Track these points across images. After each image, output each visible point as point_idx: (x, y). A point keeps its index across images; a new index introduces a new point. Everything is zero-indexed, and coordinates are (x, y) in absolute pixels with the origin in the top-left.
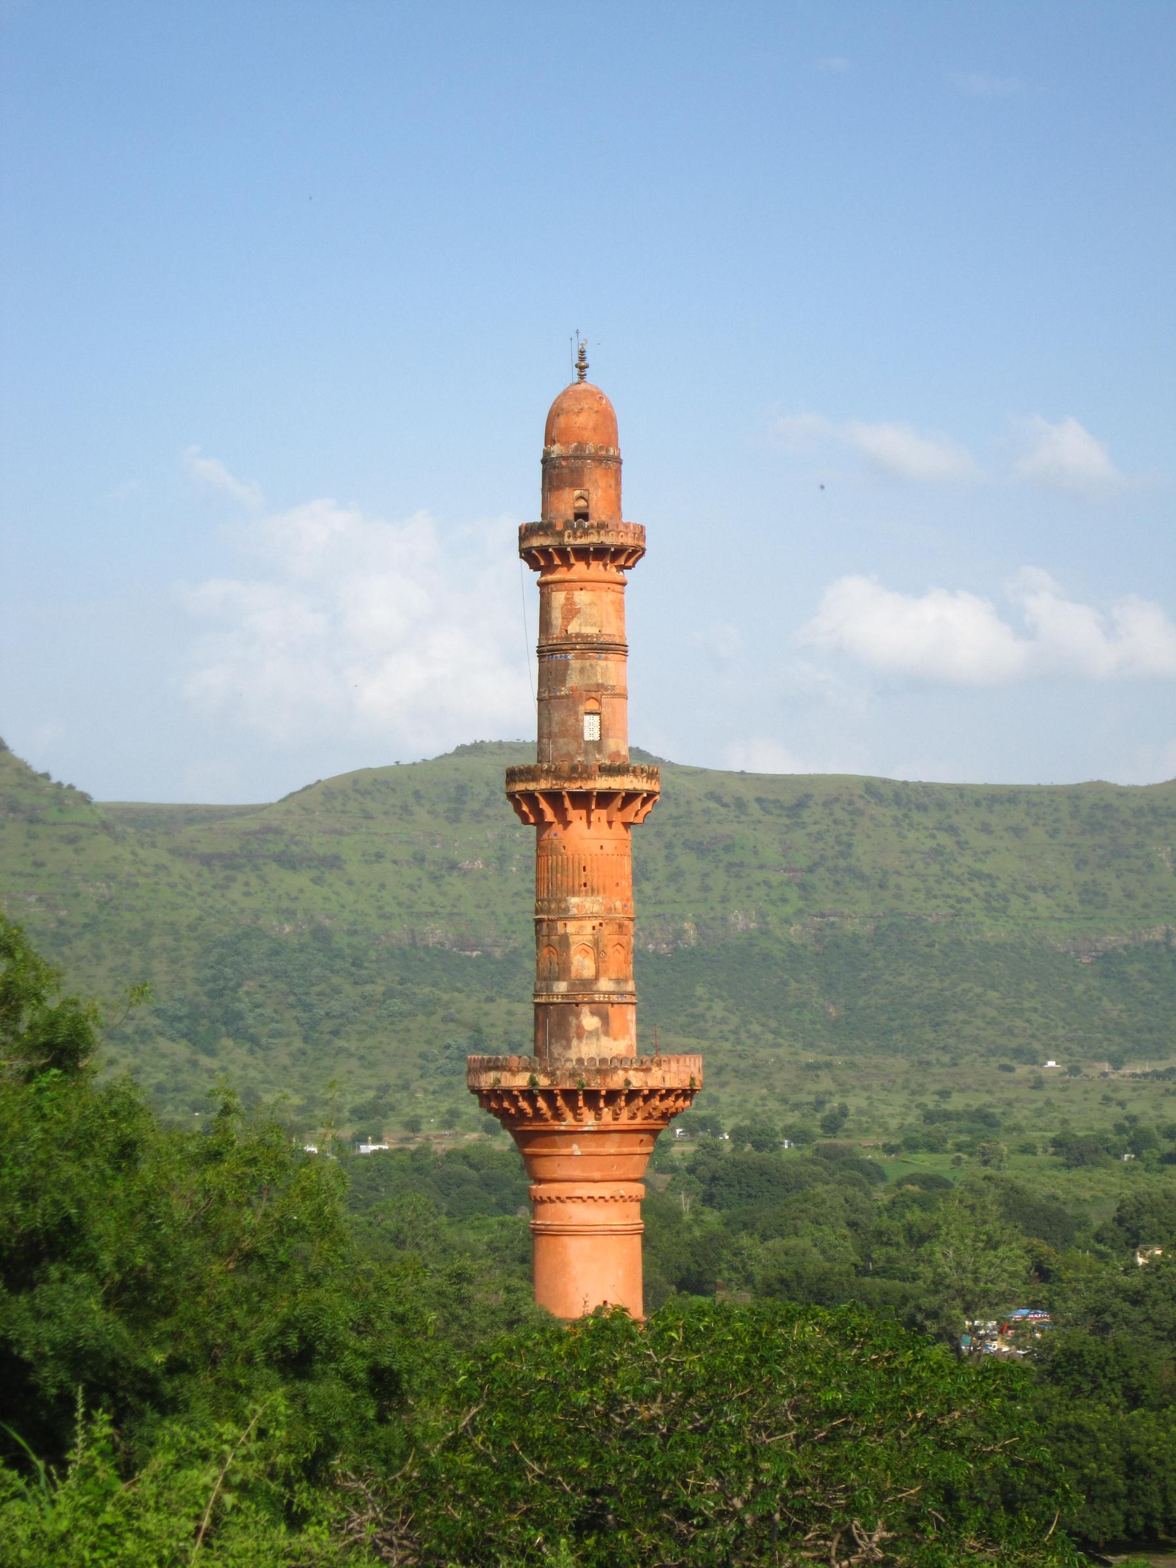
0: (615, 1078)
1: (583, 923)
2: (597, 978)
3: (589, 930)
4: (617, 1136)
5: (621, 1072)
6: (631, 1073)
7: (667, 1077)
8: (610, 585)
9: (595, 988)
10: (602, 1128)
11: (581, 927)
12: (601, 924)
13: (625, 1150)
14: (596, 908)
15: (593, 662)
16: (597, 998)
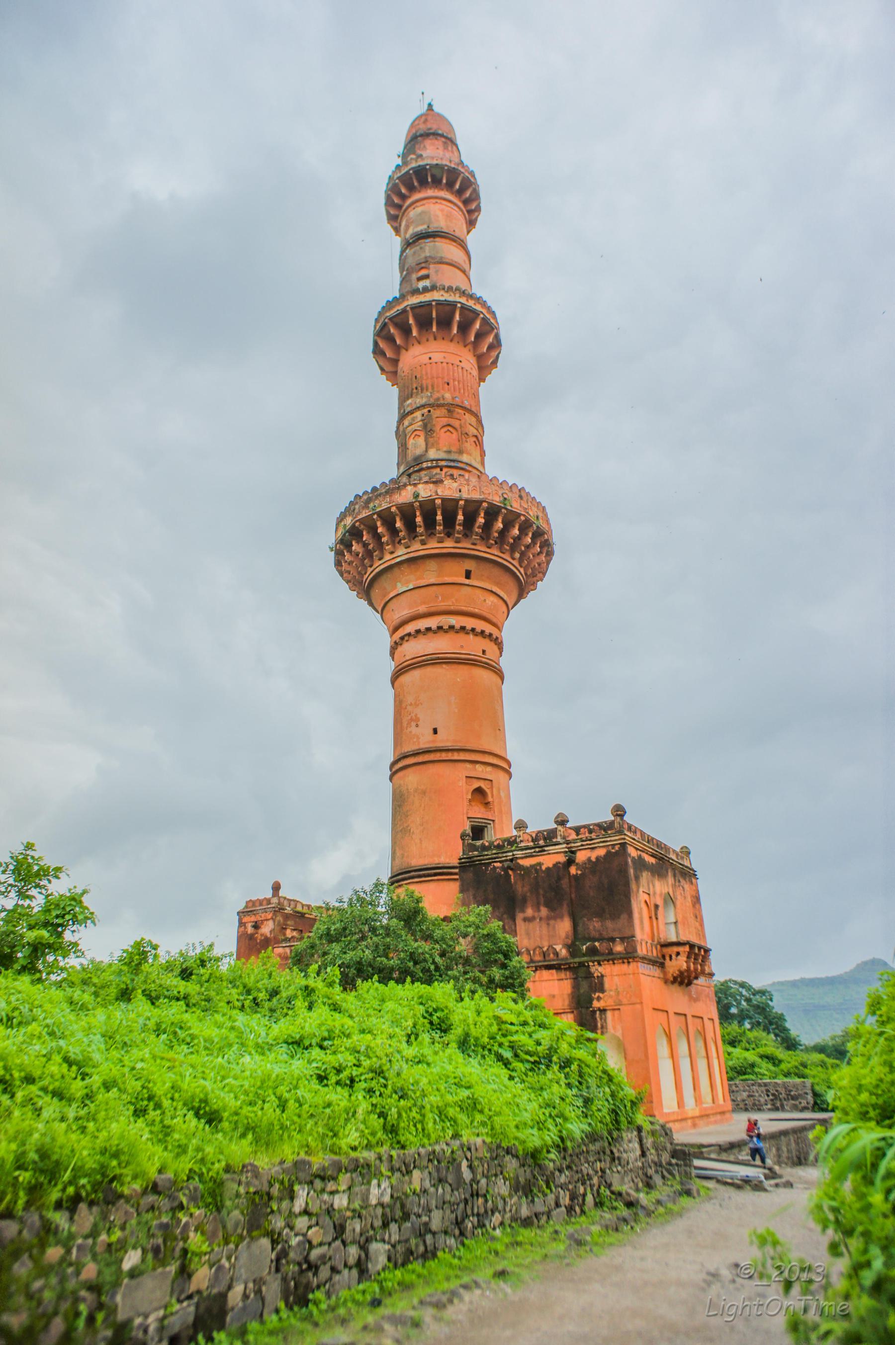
0: (404, 493)
1: (414, 415)
2: (426, 451)
3: (420, 418)
4: (432, 565)
5: (409, 488)
6: (420, 486)
7: (465, 489)
8: (439, 201)
9: (423, 460)
10: (412, 555)
11: (413, 419)
12: (429, 411)
13: (448, 580)
14: (424, 401)
15: (422, 245)
16: (425, 465)
